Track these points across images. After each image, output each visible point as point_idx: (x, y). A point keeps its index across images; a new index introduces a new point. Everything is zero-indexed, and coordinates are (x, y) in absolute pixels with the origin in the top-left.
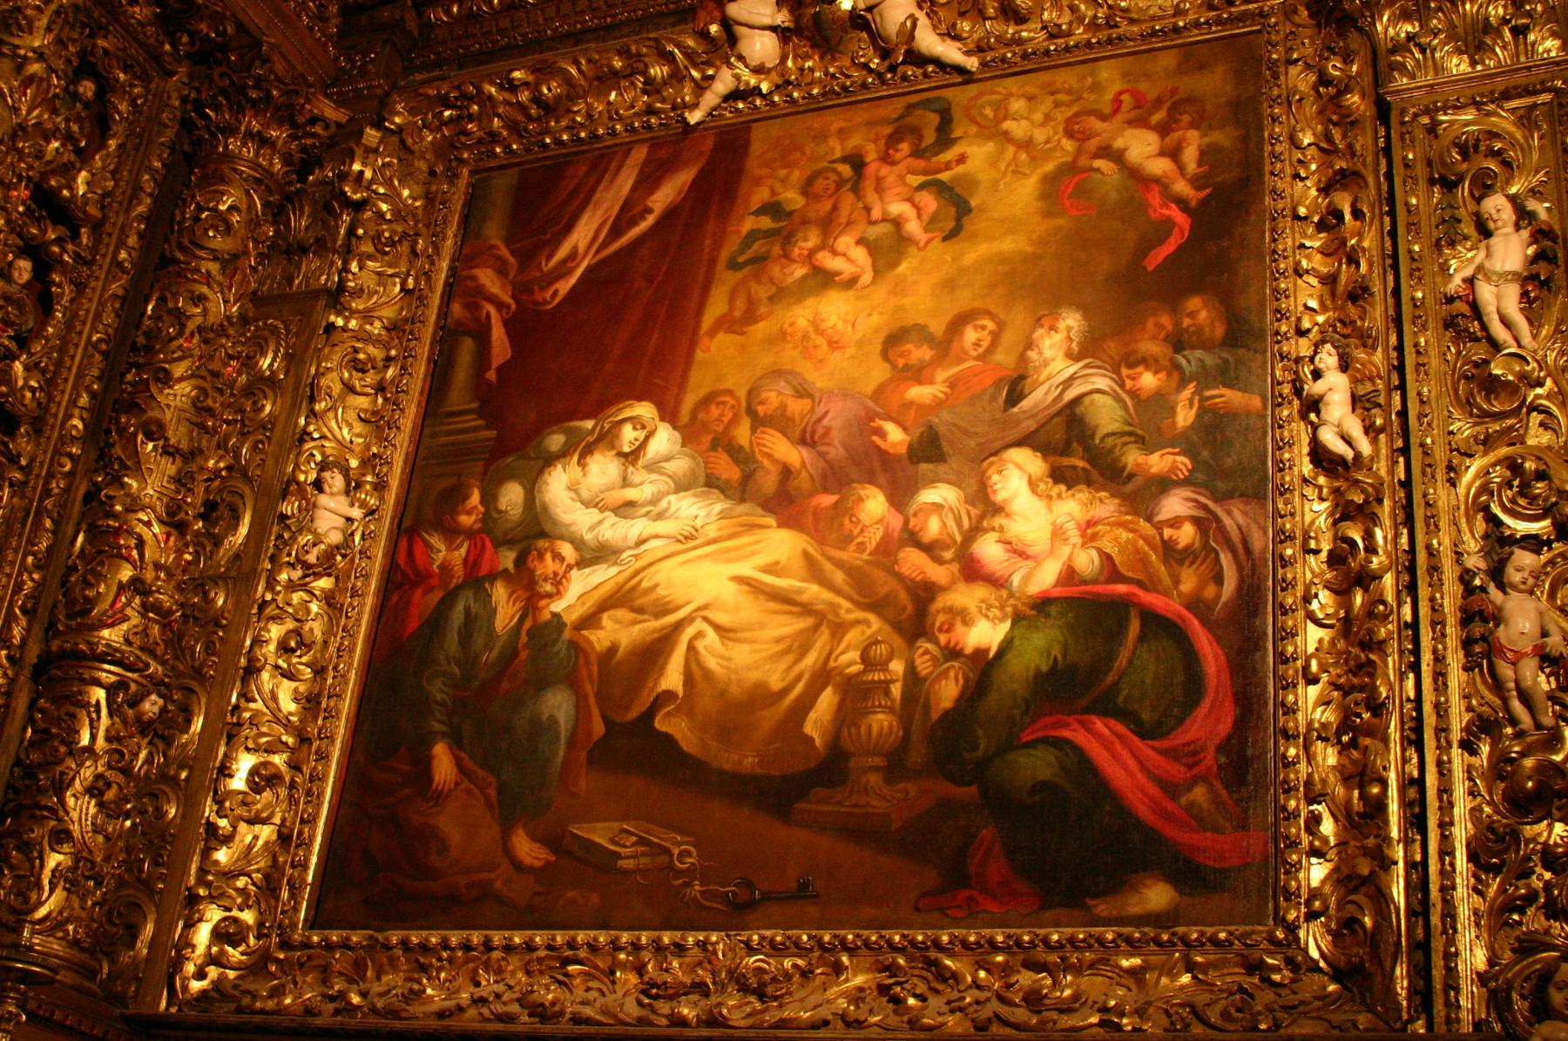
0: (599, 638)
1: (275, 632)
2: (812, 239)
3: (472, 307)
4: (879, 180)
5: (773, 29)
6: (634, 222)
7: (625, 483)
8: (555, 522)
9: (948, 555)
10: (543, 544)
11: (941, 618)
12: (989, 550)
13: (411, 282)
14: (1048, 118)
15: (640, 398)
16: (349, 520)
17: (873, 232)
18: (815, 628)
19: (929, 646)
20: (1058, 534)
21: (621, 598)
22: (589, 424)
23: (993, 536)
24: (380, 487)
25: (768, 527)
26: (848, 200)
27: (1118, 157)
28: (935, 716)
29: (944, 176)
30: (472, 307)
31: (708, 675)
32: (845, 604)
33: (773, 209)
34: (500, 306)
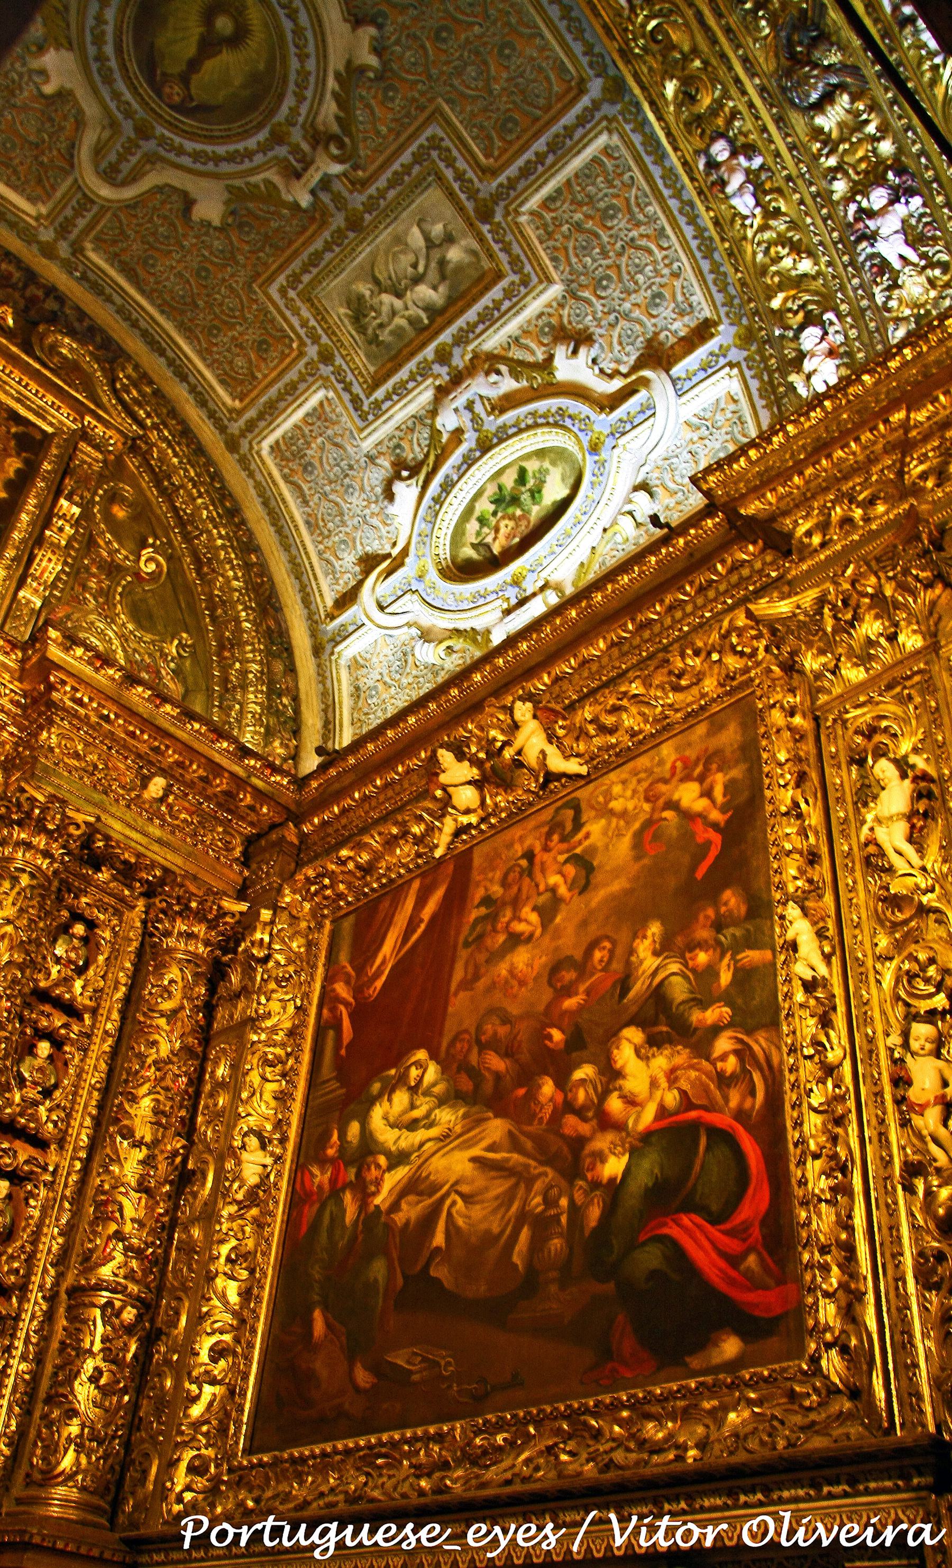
0: (399, 1218)
1: (225, 1250)
2: (508, 913)
3: (333, 1010)
4: (543, 864)
5: (469, 783)
6: (414, 931)
7: (413, 1107)
8: (376, 1142)
9: (590, 1114)
10: (370, 1159)
11: (588, 1160)
12: (615, 1104)
13: (299, 1003)
14: (635, 792)
15: (418, 1047)
16: (265, 1166)
17: (541, 900)
18: (516, 1185)
19: (581, 1183)
20: (654, 1084)
21: (412, 1187)
22: (393, 1072)
23: (616, 1094)
24: (283, 1141)
25: (488, 1119)
26: (527, 881)
27: (673, 805)
28: (587, 1233)
29: (578, 851)
30: (333, 1010)
31: (458, 1229)
32: (533, 1163)
33: (487, 901)
34: (347, 1004)
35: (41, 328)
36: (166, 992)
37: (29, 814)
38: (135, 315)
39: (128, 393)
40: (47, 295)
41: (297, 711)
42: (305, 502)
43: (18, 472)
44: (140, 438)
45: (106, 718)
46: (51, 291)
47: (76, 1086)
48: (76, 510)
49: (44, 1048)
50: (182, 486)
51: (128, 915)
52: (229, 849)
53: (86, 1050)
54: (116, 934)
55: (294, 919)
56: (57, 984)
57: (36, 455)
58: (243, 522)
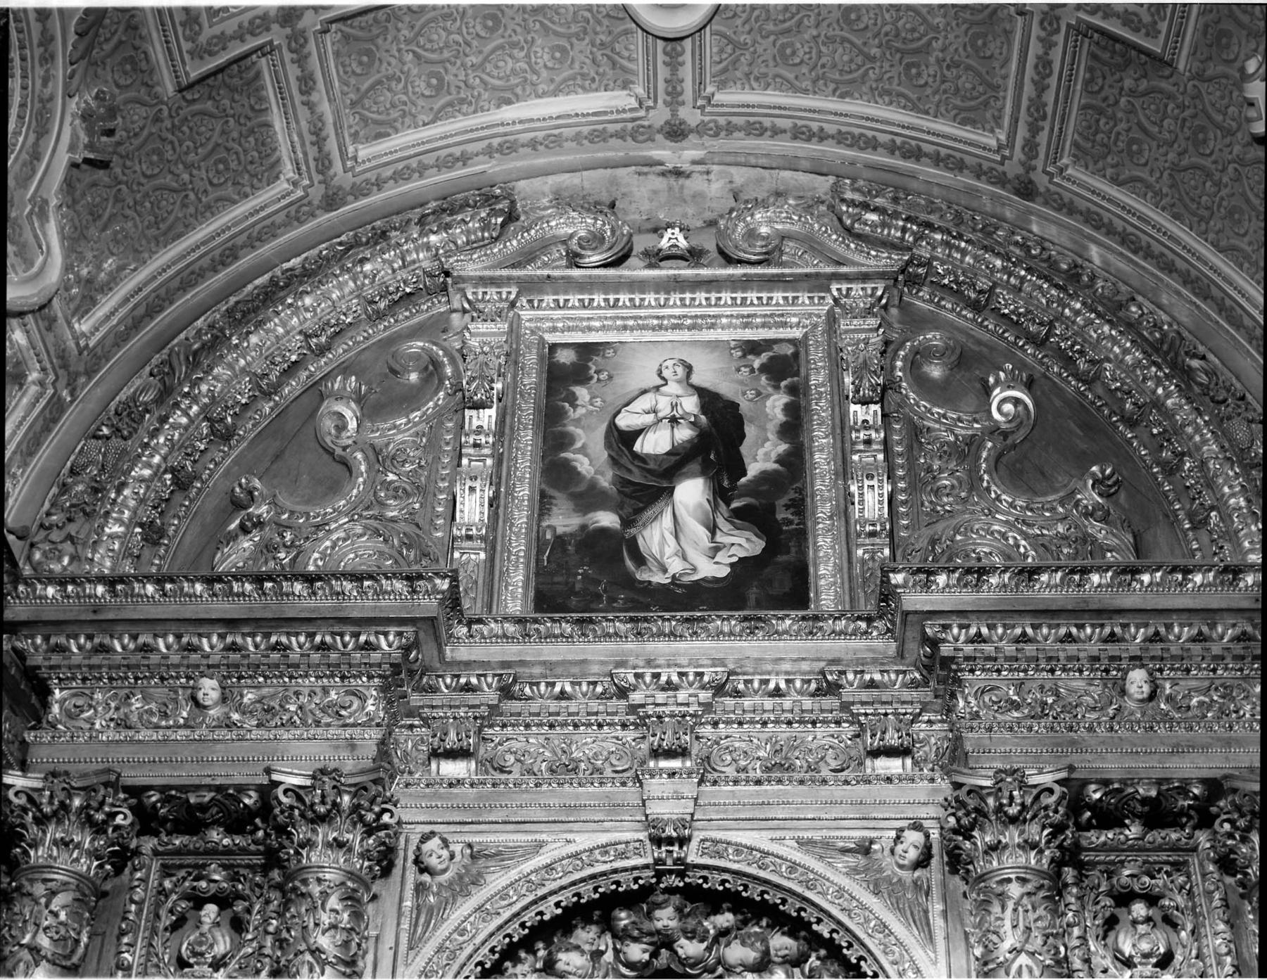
38: (815, 126)
43: (788, 408)
44: (909, 263)
57: (797, 374)
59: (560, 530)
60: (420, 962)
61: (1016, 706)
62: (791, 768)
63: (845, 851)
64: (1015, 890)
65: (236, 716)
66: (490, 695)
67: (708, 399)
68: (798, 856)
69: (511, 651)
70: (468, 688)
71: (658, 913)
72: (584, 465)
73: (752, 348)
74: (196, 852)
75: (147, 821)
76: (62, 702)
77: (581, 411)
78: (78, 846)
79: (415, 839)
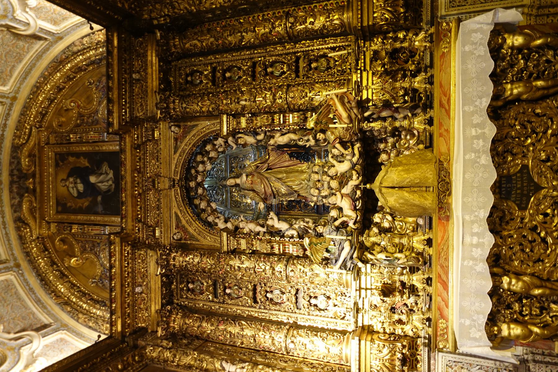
35: (25, 172)
36: (195, 45)
37: (165, 112)
39: (24, 138)
40: (14, 175)
41: (86, 36)
42: (14, 66)
43: (72, 156)
44: (36, 127)
45: (125, 102)
46: (11, 174)
47: (234, 60)
48: (71, 136)
49: (228, 75)
50: (40, 106)
51: (179, 66)
52: (142, 43)
53: (223, 62)
54: (186, 67)
55: (151, 11)
56: (209, 79)
57: (64, 154)
58: (37, 82)
59: (102, 209)
60: (202, 239)
61: (141, 105)
62: (157, 156)
63: (176, 144)
64: (184, 105)
65: (145, 283)
66: (140, 225)
67: (69, 175)
68: (178, 154)
69: (130, 220)
70: (139, 230)
71: (191, 186)
72: (86, 204)
73: (57, 165)
74: (177, 291)
75: (170, 303)
76: (141, 324)
77: (73, 205)
78: (175, 318)
79: (174, 241)
